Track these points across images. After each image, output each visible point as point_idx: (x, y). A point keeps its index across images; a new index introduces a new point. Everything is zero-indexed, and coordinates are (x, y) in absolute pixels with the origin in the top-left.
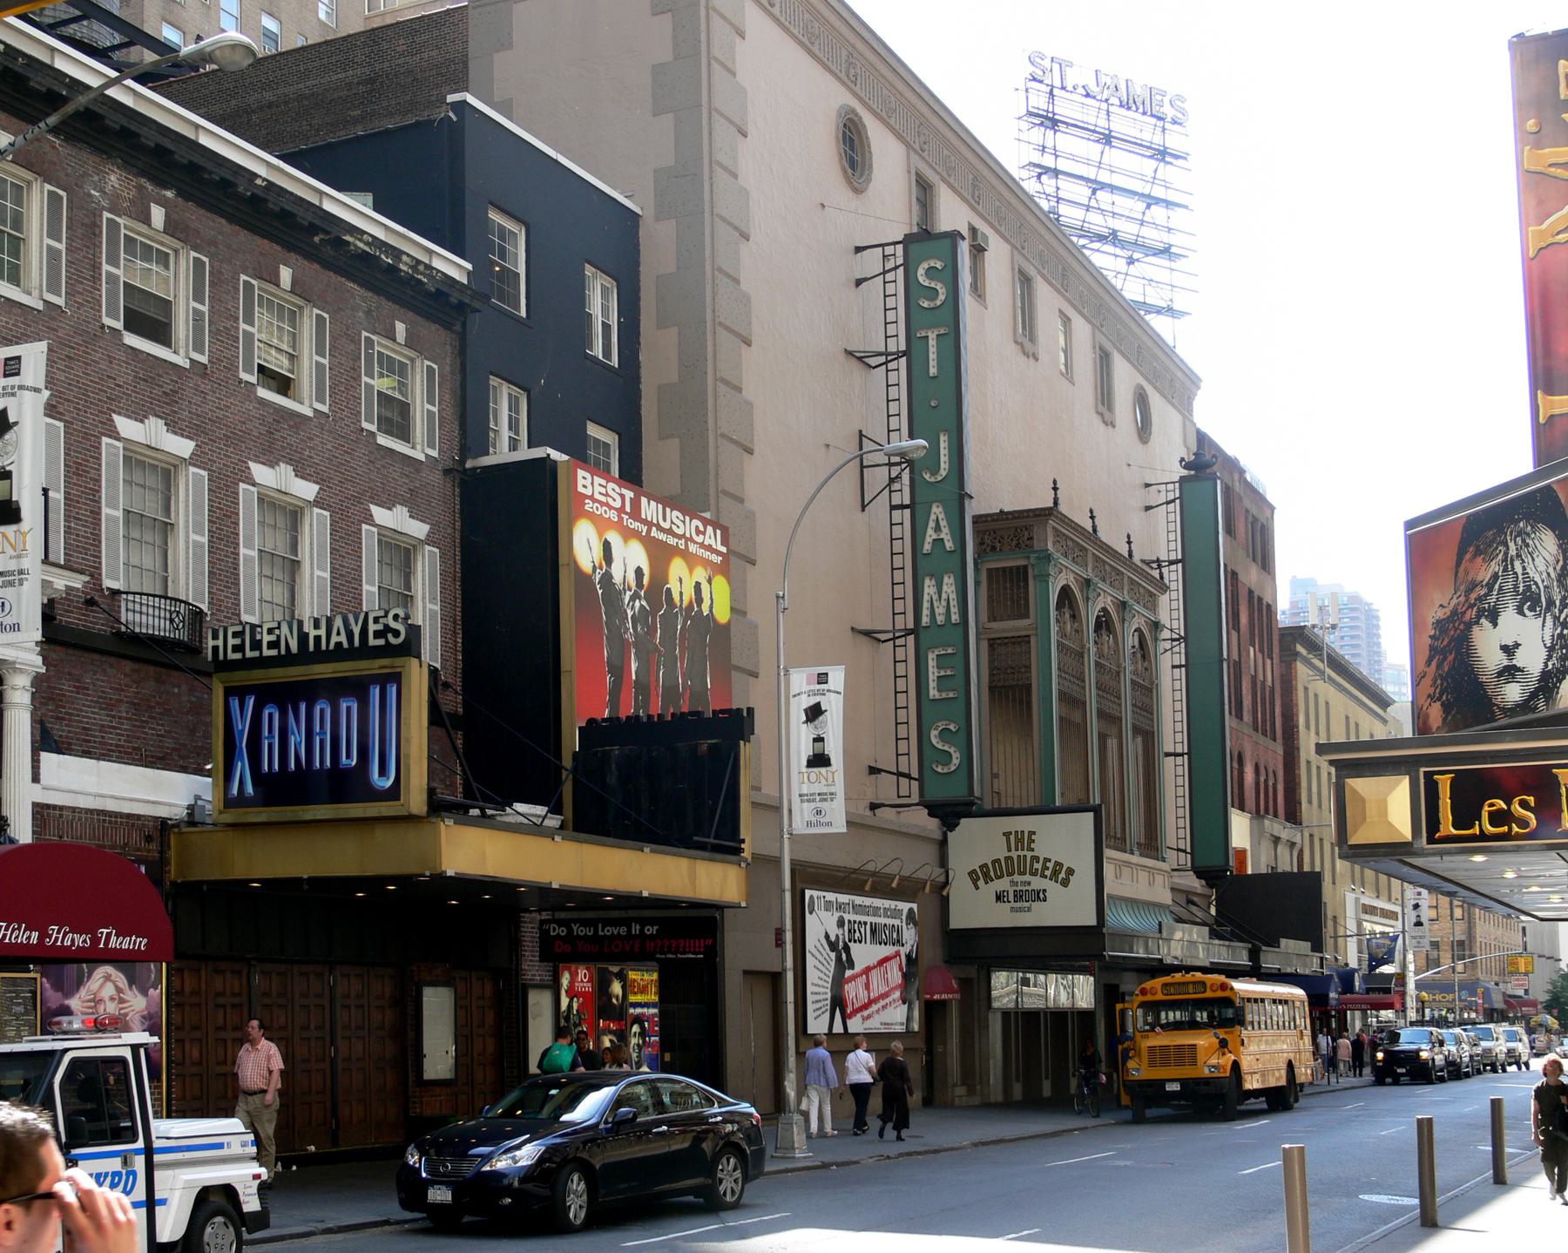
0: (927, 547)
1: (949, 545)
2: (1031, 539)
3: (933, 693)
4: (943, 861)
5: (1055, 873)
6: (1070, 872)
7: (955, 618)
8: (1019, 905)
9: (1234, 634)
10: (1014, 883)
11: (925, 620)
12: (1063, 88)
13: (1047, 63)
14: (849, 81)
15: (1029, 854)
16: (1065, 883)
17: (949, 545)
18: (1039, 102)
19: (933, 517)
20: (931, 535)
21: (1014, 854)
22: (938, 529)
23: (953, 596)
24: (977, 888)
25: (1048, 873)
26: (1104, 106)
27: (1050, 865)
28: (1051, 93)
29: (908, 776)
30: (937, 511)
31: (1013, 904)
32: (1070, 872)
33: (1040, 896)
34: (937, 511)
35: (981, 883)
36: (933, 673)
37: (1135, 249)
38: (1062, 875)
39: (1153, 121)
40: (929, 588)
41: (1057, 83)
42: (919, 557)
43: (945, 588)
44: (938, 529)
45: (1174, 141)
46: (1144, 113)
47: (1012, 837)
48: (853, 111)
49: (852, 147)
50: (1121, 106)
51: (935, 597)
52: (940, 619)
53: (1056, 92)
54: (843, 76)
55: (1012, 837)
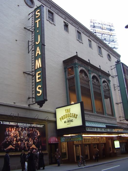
0: (36, 56)
1: (40, 54)
2: (73, 62)
3: (38, 81)
4: (56, 117)
5: (74, 116)
6: (77, 115)
7: (41, 66)
8: (68, 123)
10: (67, 119)
11: (36, 68)
15: (69, 113)
16: (76, 118)
17: (40, 54)
18: (92, 24)
19: (37, 50)
20: (37, 53)
21: (67, 114)
22: (38, 51)
23: (40, 63)
24: (61, 121)
25: (73, 116)
27: (73, 115)
28: (94, 23)
29: (34, 98)
30: (38, 49)
31: (67, 123)
32: (77, 115)
33: (72, 121)
34: (38, 49)
35: (62, 120)
36: (37, 77)
38: (76, 116)
40: (37, 61)
43: (39, 62)
44: (38, 51)
45: (112, 28)
47: (66, 110)
51: (38, 64)
52: (38, 67)
55: (66, 110)
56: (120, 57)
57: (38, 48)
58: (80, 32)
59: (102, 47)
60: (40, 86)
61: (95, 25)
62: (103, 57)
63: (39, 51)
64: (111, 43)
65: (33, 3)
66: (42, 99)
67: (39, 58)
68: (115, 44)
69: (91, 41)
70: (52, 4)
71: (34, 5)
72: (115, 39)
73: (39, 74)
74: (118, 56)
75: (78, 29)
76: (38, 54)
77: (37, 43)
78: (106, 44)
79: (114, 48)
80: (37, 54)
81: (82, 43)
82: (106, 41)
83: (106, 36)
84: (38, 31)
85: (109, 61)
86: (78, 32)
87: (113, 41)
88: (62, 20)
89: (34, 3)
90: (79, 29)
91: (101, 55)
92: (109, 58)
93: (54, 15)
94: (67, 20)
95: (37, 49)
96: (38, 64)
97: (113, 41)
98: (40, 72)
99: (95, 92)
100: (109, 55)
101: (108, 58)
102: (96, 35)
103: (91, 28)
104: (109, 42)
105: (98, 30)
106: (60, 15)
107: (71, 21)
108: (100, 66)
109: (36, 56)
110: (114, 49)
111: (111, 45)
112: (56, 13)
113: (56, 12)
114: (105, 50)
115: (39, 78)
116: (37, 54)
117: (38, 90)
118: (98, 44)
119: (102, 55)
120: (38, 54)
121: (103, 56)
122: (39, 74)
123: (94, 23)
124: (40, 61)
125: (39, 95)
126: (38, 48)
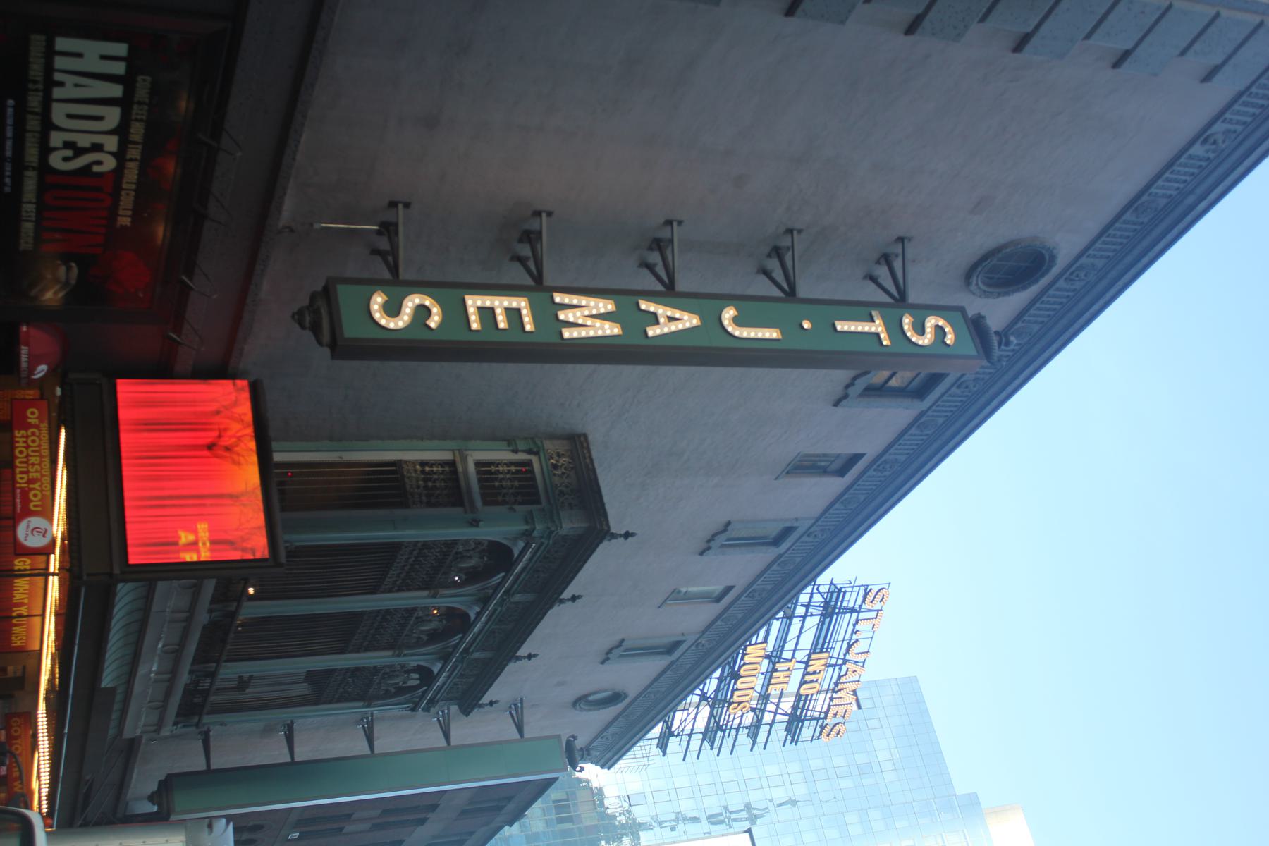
1: (652, 332)
3: (474, 302)
7: (567, 334)
9: (367, 826)
11: (558, 298)
12: (857, 621)
13: (877, 606)
14: (1070, 271)
17: (652, 332)
18: (851, 600)
19: (677, 314)
20: (662, 311)
22: (671, 319)
26: (840, 662)
28: (853, 610)
30: (689, 321)
34: (689, 321)
36: (500, 303)
37: (719, 702)
39: (825, 709)
41: (862, 616)
42: (632, 299)
43: (598, 323)
44: (671, 319)
45: (807, 731)
46: (831, 699)
48: (1048, 271)
49: (1015, 266)
50: (839, 678)
52: (562, 316)
53: (855, 615)
54: (1084, 260)
56: (602, 767)
57: (695, 321)
58: (784, 546)
59: (672, 663)
60: (434, 322)
61: (846, 620)
62: (603, 663)
63: (673, 327)
64: (705, 711)
65: (998, 290)
66: (352, 329)
67: (623, 328)
68: (697, 738)
69: (718, 599)
70: (987, 396)
71: (986, 294)
72: (729, 742)
73: (514, 314)
74: (607, 762)
75: (808, 533)
76: (654, 319)
77: (728, 314)
78: (703, 682)
79: (669, 728)
80: (652, 308)
81: (709, 548)
82: (720, 679)
83: (758, 682)
84: (806, 325)
85: (573, 698)
86: (788, 531)
87: (719, 728)
88: (870, 446)
89: (999, 295)
90: (805, 538)
91: (619, 651)
92: (590, 698)
93: (907, 402)
94: (871, 472)
95: (686, 316)
96: (578, 312)
97: (719, 728)
98: (528, 327)
99: (354, 618)
100: (615, 698)
101: (595, 693)
102: (773, 617)
103: (824, 589)
104: (715, 699)
105: (804, 632)
106: (906, 437)
107: (862, 498)
108: (530, 657)
109: (644, 305)
110: (657, 731)
111: (691, 716)
112: (922, 414)
113: (930, 413)
114: (656, 679)
115: (487, 314)
116: (652, 308)
117: (412, 302)
118: (696, 643)
119: (621, 656)
120: (654, 319)
121: (607, 666)
122: (514, 314)
123: (853, 610)
124: (600, 333)
125: (378, 300)
126: (695, 321)
